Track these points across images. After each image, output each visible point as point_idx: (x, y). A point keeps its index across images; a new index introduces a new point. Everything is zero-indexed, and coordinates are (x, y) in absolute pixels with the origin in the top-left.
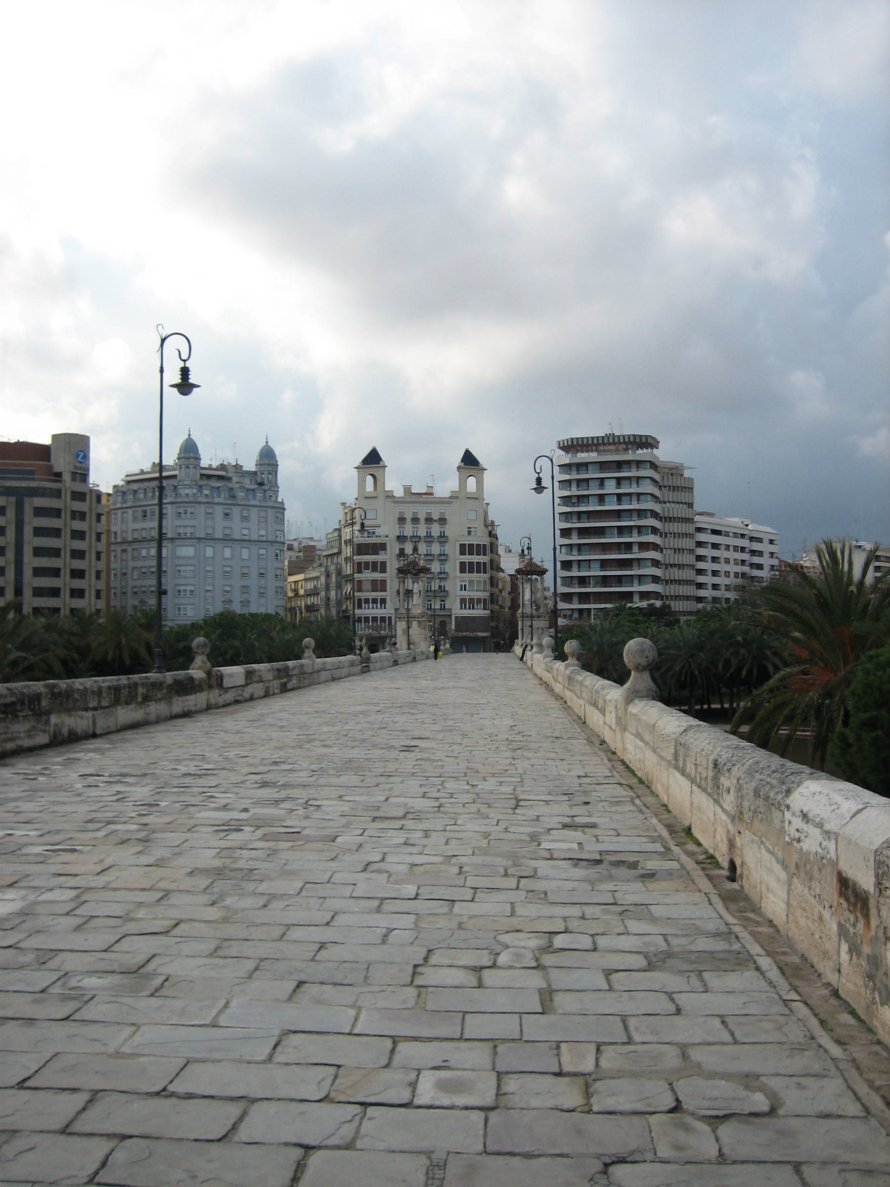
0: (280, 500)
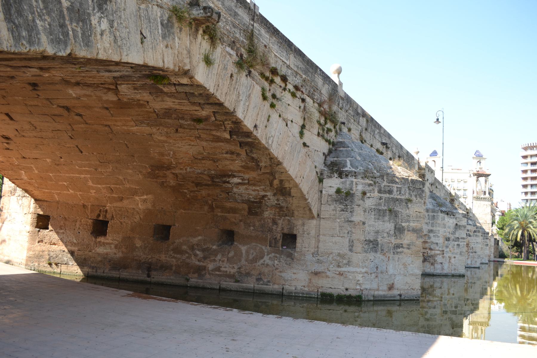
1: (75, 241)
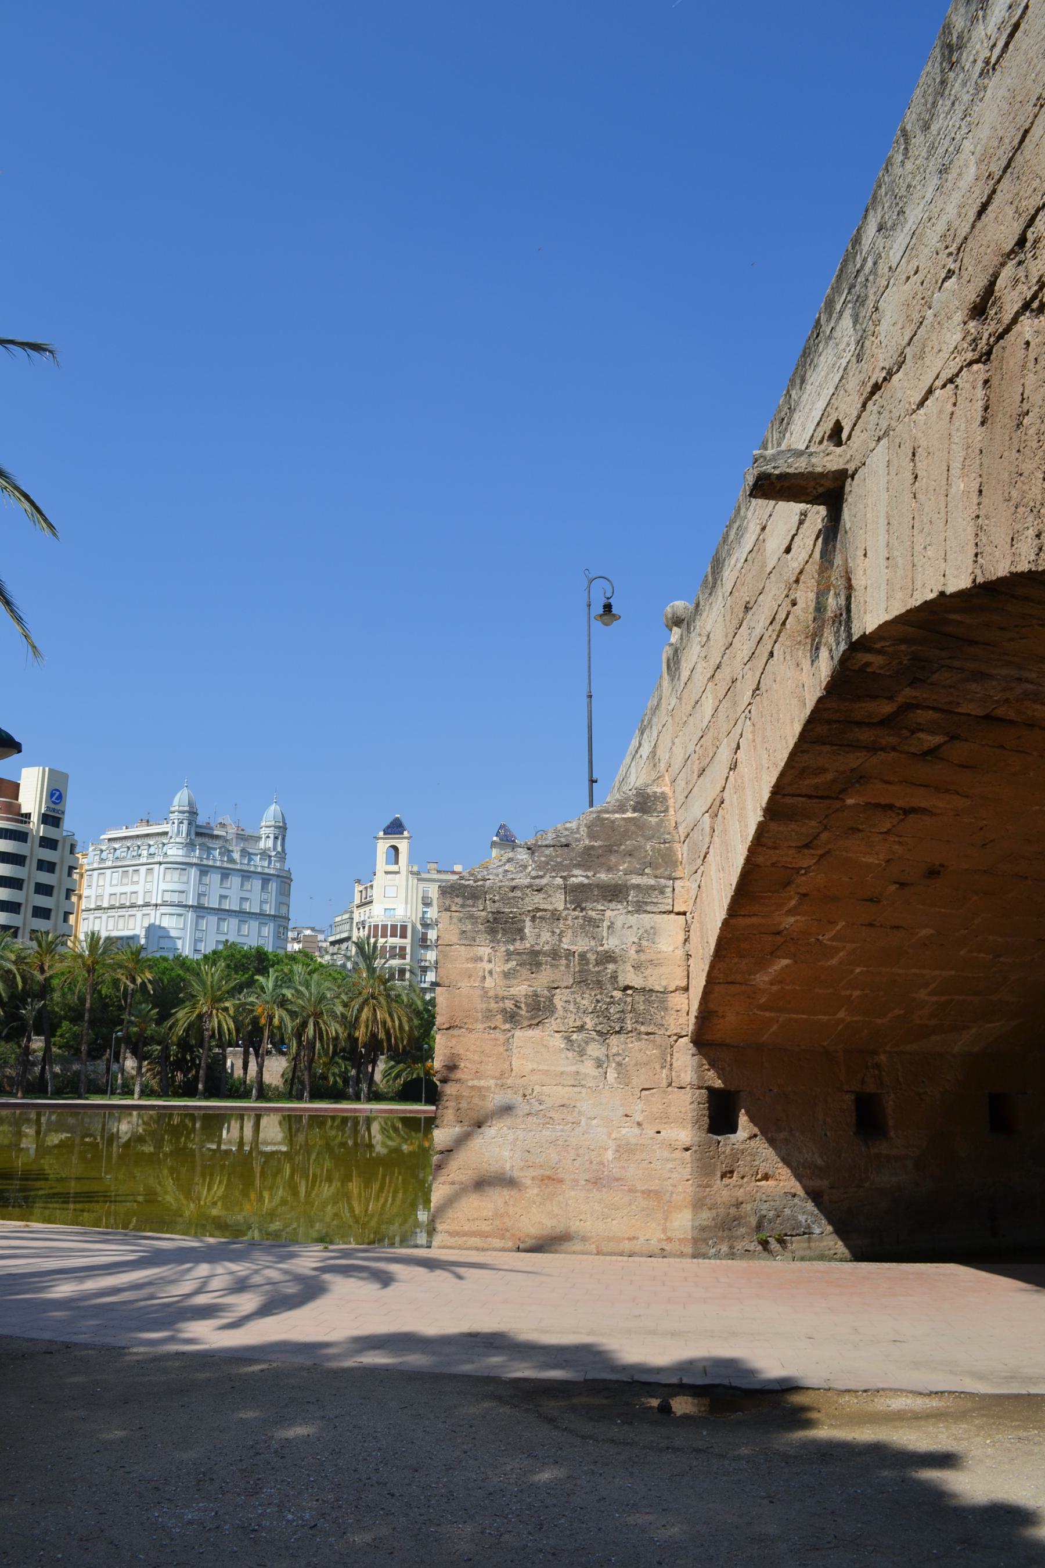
1: (820, 1162)
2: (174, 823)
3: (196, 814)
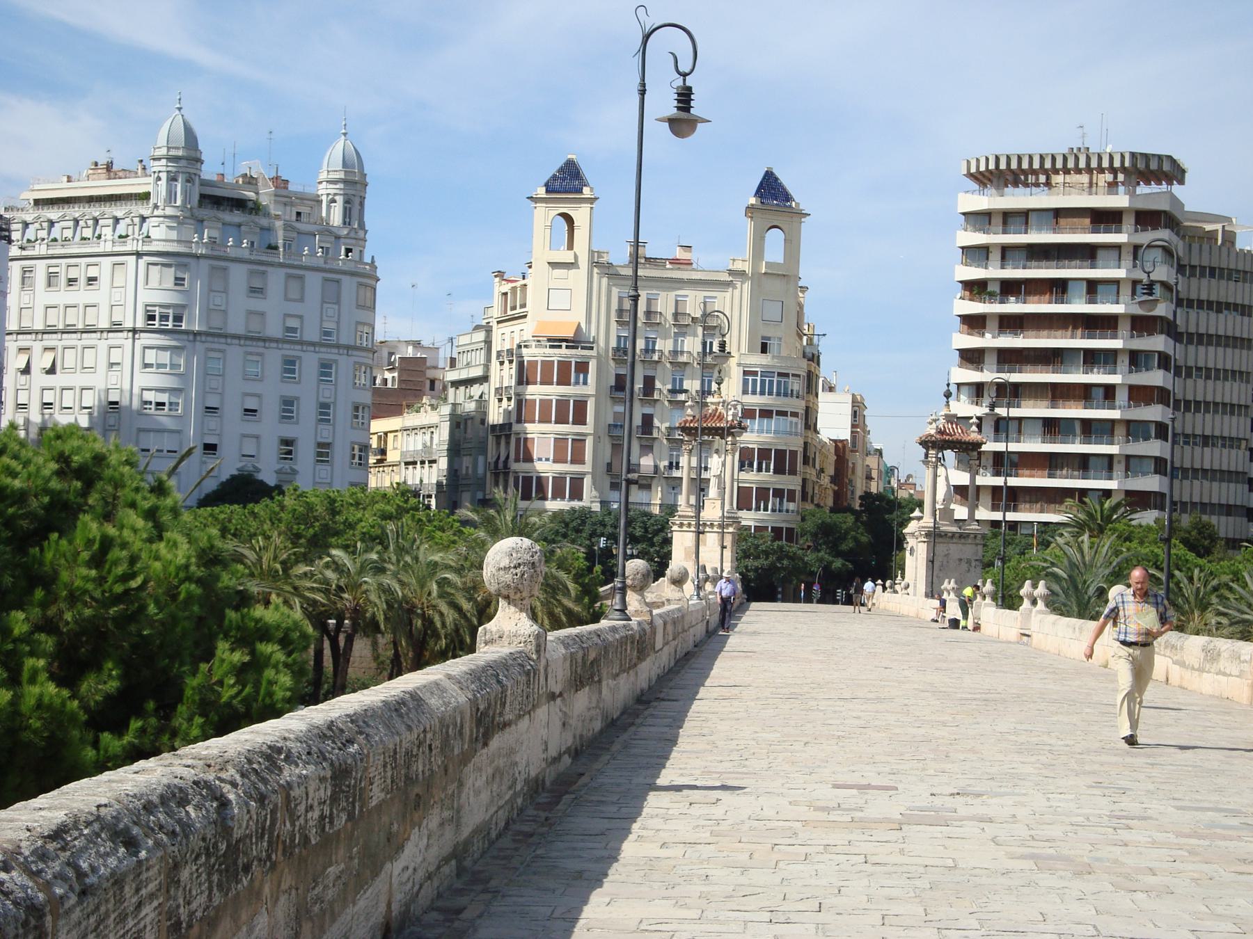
0: (367, 259)
2: (159, 179)
3: (199, 161)
